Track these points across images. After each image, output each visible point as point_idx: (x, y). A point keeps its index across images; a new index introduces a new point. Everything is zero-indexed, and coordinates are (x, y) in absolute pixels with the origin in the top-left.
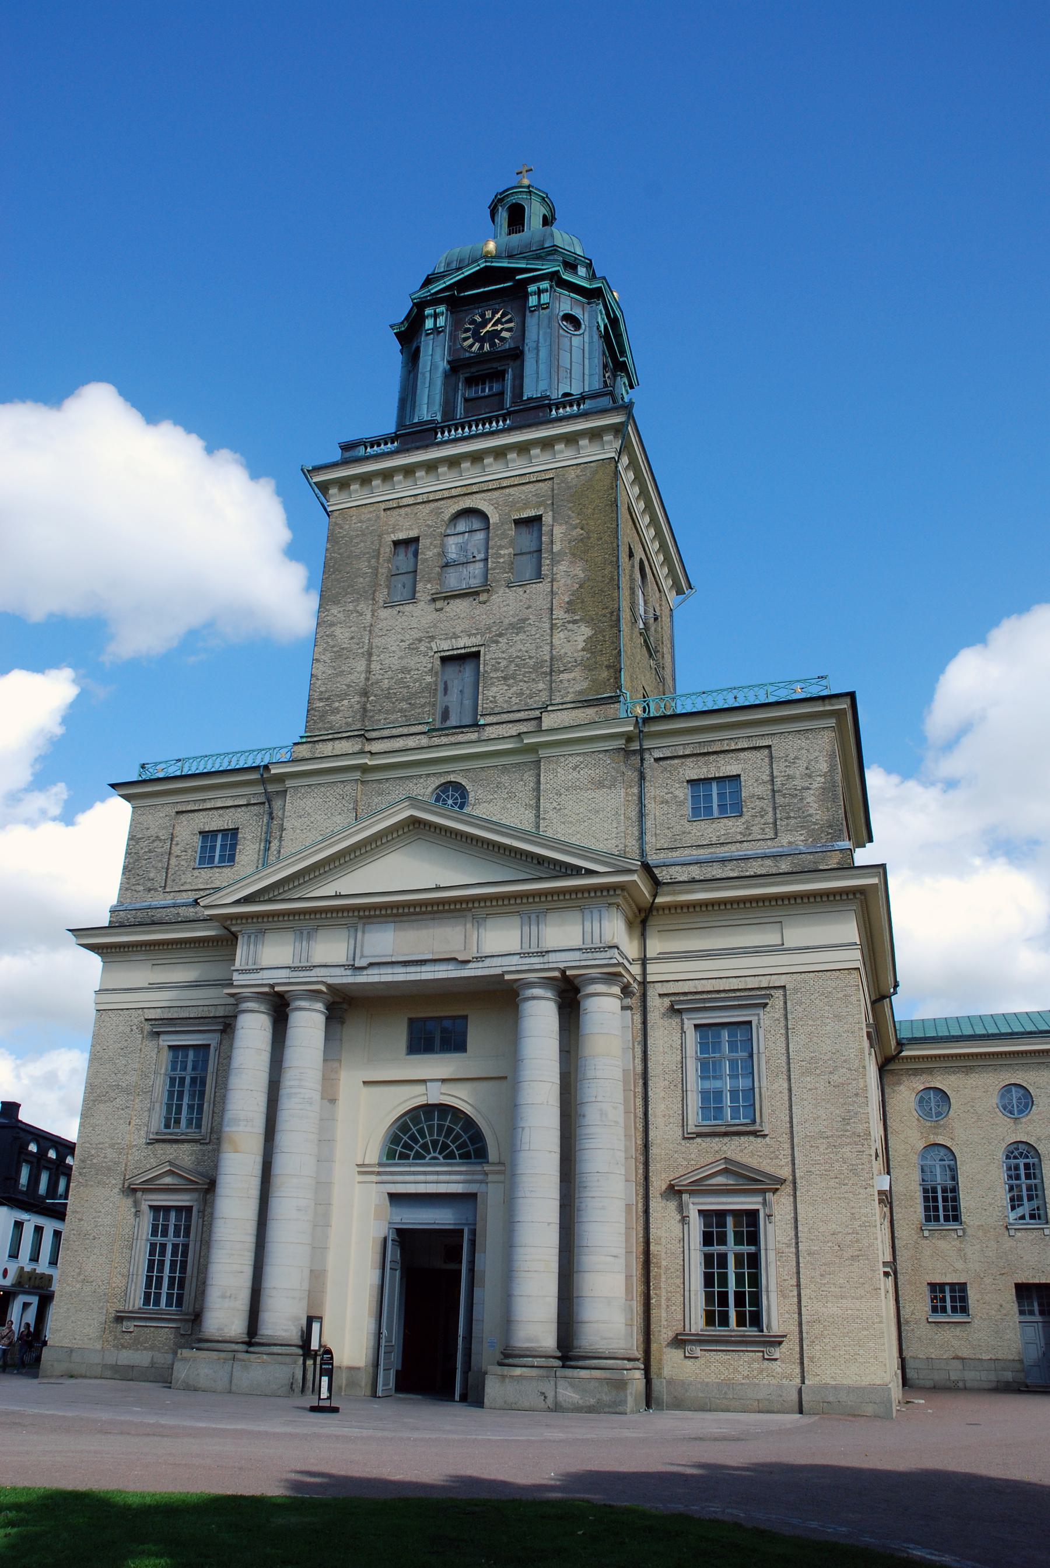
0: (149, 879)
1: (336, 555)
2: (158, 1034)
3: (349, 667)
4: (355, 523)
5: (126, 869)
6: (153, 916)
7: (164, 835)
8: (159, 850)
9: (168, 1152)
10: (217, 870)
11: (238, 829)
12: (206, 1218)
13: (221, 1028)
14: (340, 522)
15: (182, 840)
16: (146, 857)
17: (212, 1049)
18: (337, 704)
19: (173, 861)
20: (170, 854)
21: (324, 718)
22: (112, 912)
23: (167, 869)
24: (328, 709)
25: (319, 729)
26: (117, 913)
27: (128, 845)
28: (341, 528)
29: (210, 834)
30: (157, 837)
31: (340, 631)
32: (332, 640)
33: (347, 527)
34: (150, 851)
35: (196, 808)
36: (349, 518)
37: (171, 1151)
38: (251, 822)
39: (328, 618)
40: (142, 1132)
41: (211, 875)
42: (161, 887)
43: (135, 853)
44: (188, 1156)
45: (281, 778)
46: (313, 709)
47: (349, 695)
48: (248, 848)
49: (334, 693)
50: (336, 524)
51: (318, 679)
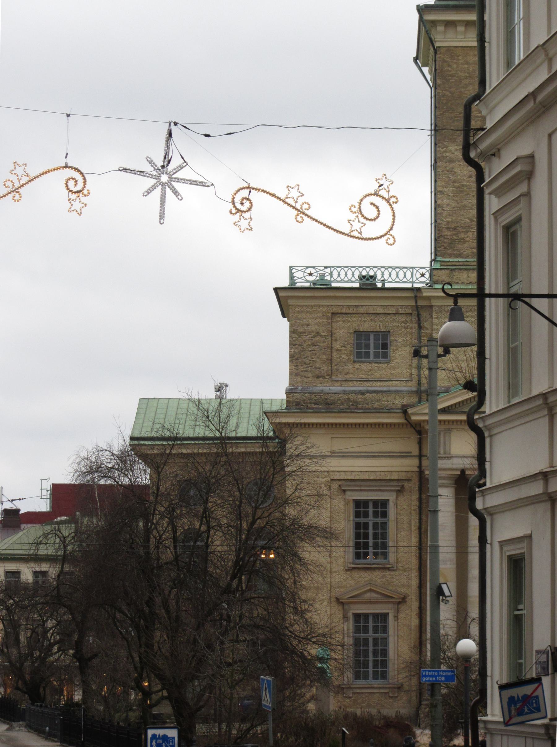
0: (316, 368)
1: (447, 93)
2: (344, 491)
3: (470, 203)
4: (462, 64)
5: (292, 358)
6: (326, 399)
7: (323, 331)
8: (321, 344)
9: (363, 576)
10: (376, 365)
11: (389, 332)
12: (399, 621)
13: (399, 489)
14: (448, 60)
15: (340, 337)
16: (310, 349)
17: (391, 504)
18: (462, 235)
19: (335, 354)
20: (331, 348)
21: (453, 246)
22: (289, 393)
23: (331, 360)
24: (456, 238)
25: (450, 255)
26: (292, 395)
27: (290, 337)
28: (449, 66)
29: (363, 333)
30: (318, 333)
31: (459, 169)
32: (453, 175)
33: (455, 66)
34: (313, 344)
35: (350, 312)
36: (456, 57)
37: (365, 576)
38: (400, 328)
39: (447, 154)
40: (339, 563)
41: (370, 368)
42: (327, 375)
43: (299, 345)
44: (380, 579)
45: (429, 298)
46: (442, 236)
47: (472, 228)
48: (400, 349)
49: (459, 224)
50: (444, 61)
51: (443, 210)
